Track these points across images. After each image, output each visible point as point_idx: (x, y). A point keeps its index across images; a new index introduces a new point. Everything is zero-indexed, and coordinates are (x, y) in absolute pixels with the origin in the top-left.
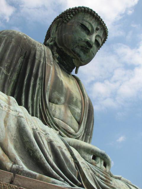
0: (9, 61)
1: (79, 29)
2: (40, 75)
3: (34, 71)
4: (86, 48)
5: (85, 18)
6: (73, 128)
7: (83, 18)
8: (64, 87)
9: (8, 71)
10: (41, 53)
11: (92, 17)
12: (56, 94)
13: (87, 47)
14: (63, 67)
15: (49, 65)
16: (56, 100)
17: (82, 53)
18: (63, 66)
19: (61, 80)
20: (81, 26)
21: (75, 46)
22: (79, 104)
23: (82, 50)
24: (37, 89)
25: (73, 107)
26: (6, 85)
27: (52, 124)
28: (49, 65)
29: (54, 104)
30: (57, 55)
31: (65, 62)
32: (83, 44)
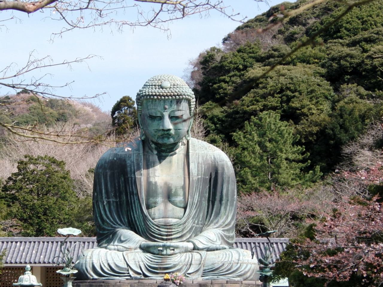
0: (113, 190)
1: (149, 121)
2: (135, 192)
3: (131, 190)
4: (165, 134)
5: (149, 108)
6: (176, 218)
7: (147, 108)
8: (159, 187)
9: (116, 198)
10: (131, 168)
11: (154, 100)
12: (152, 200)
13: (166, 133)
14: (164, 154)
15: (139, 177)
16: (153, 205)
17: (166, 139)
18: (163, 152)
19: (156, 183)
20: (149, 117)
21: (156, 138)
22: (181, 192)
23: (163, 138)
24: (136, 204)
25: (173, 199)
26: (119, 210)
27: (153, 227)
28: (139, 177)
29: (153, 209)
30: (153, 146)
31: (163, 149)
32: (160, 133)
